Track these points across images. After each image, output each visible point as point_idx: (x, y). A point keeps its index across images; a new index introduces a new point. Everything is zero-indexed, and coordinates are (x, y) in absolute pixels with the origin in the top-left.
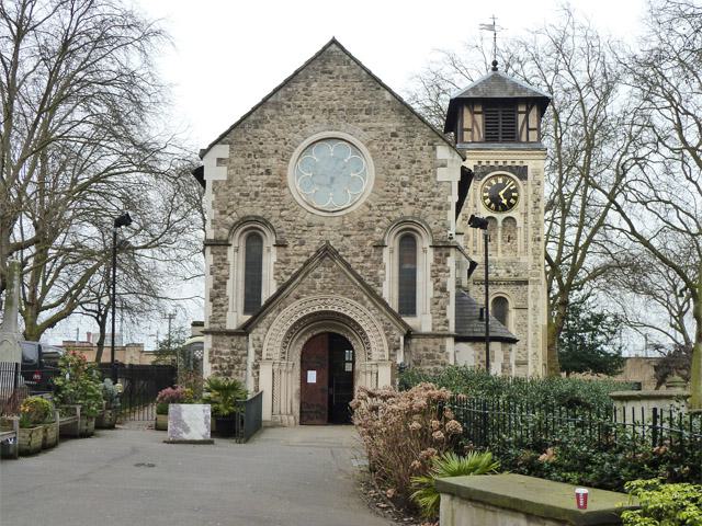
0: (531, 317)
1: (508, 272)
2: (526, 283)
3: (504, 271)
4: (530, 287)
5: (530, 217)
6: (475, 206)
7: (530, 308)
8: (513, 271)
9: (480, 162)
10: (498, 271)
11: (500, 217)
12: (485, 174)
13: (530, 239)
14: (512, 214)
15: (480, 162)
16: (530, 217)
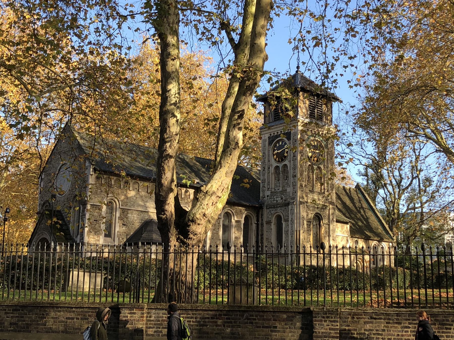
0: (290, 226)
1: (282, 199)
2: (288, 204)
3: (280, 199)
4: (290, 206)
5: (292, 162)
6: (269, 161)
7: (290, 219)
8: (284, 198)
9: (271, 134)
10: (278, 199)
11: (281, 165)
12: (273, 141)
13: (291, 176)
14: (286, 162)
15: (271, 134)
16: (292, 162)
